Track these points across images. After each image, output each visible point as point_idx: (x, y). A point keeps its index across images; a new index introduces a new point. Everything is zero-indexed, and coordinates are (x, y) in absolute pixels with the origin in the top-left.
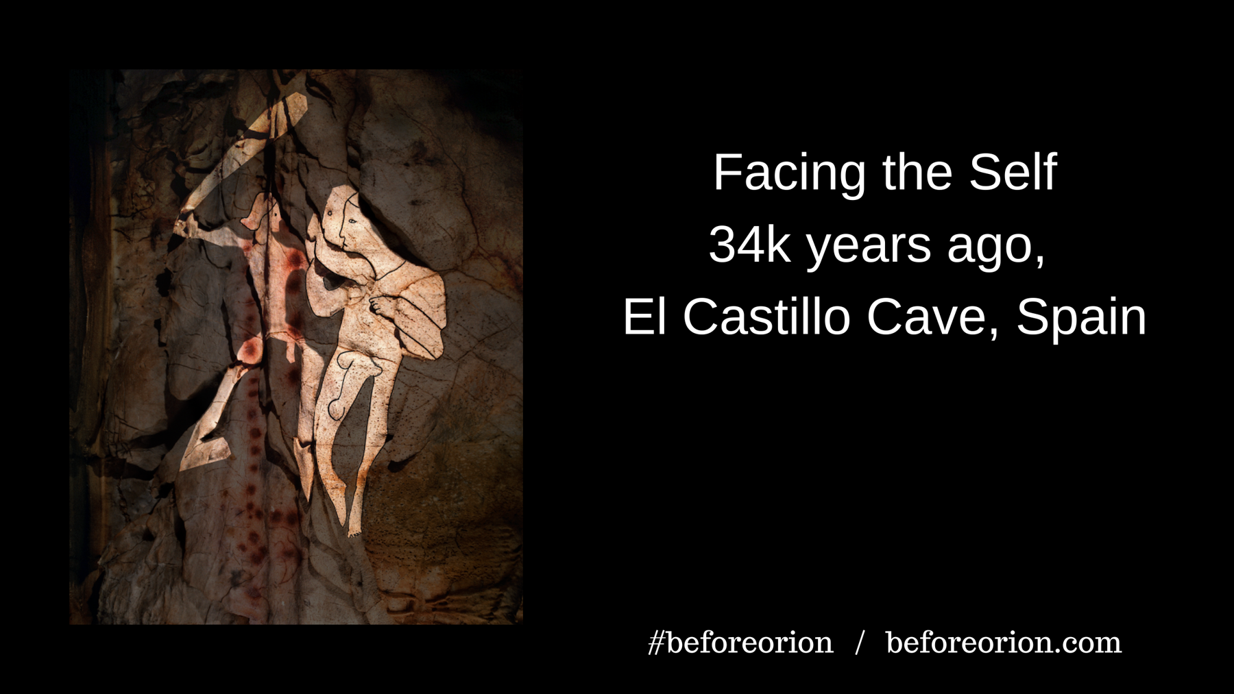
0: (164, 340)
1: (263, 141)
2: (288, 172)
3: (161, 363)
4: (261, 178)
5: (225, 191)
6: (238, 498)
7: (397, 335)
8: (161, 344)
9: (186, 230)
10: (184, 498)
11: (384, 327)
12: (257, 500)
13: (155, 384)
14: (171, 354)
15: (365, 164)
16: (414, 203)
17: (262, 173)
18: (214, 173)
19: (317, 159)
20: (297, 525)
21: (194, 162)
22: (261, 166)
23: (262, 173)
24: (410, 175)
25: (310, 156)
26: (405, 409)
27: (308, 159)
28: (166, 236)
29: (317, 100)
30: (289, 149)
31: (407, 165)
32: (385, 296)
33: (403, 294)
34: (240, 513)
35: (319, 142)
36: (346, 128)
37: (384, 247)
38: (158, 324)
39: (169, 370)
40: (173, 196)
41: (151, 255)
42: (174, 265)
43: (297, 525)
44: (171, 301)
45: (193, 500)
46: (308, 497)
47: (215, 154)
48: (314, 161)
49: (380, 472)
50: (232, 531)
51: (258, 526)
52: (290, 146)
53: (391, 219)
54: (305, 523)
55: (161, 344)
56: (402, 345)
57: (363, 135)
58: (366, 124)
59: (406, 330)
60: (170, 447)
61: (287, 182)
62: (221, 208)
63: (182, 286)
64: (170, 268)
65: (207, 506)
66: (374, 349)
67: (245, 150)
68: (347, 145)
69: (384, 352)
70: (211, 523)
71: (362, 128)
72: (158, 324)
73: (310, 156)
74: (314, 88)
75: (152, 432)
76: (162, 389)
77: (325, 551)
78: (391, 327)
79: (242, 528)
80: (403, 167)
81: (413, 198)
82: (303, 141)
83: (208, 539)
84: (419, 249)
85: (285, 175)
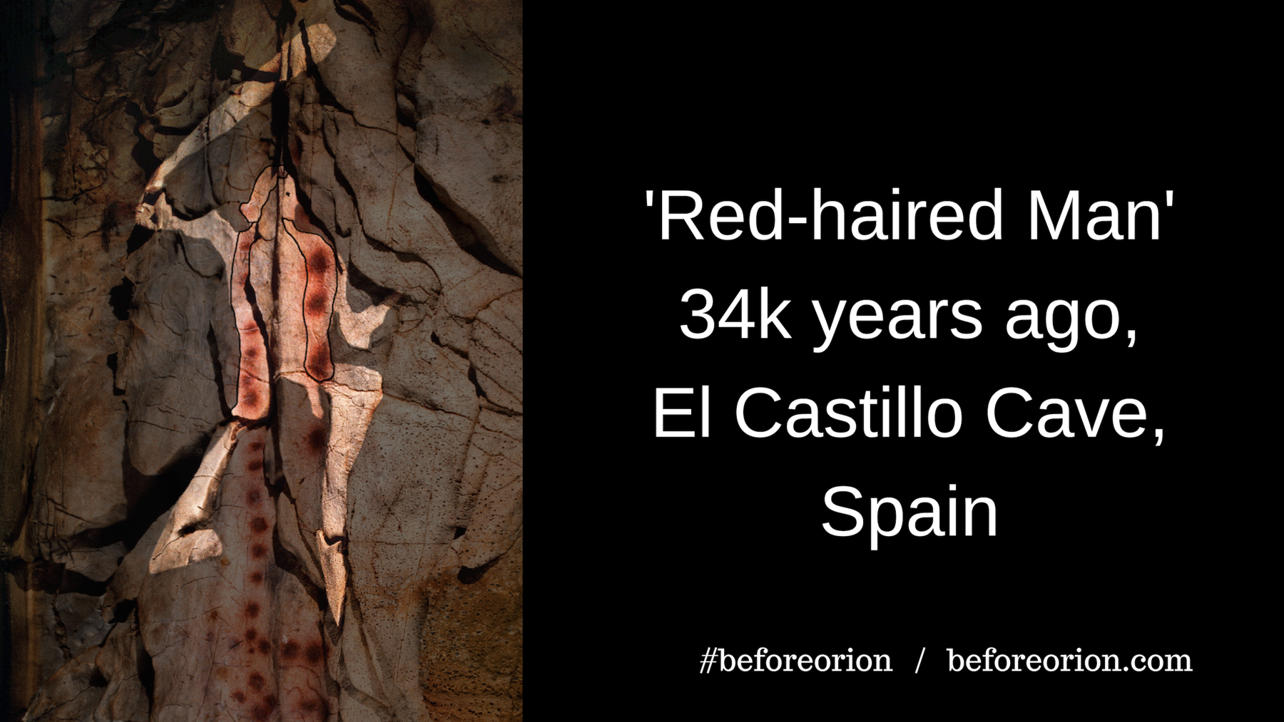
0: (121, 386)
1: (270, 86)
2: (307, 132)
3: (117, 420)
4: (268, 142)
5: (213, 162)
6: (233, 623)
7: (472, 376)
8: (118, 392)
9: (155, 219)
10: (152, 622)
11: (453, 365)
12: (261, 625)
13: (109, 451)
14: (133, 407)
15: (422, 122)
16: (497, 179)
17: (269, 135)
18: (196, 132)
19: (351, 113)
20: (321, 663)
21: (167, 118)
22: (268, 123)
23: (269, 135)
24: (490, 138)
25: (341, 108)
26: (484, 488)
27: (337, 114)
28: (125, 229)
29: (352, 26)
30: (310, 99)
31: (486, 122)
32: (454, 317)
33: (482, 315)
34: (235, 645)
35: (353, 89)
36: (395, 67)
37: (454, 244)
38: (113, 362)
39: (130, 430)
40: (136, 168)
41: (102, 258)
42: (137, 272)
43: (321, 663)
44: (132, 327)
45: (165, 625)
46: (338, 619)
47: (199, 106)
48: (347, 117)
49: (446, 583)
50: (223, 672)
51: (262, 664)
52: (311, 94)
53: (462, 204)
54: (334, 660)
55: (118, 392)
56: (480, 392)
57: (421, 77)
58: (425, 61)
59: (486, 369)
60: (130, 545)
61: (307, 147)
62: (208, 186)
63: (148, 304)
64: (131, 277)
65: (186, 634)
66: (437, 399)
67: (243, 98)
68: (396, 92)
69: (453, 404)
70: (192, 660)
71: (419, 67)
72: (113, 362)
73: (341, 108)
74: (346, 7)
75: (105, 523)
76: (119, 458)
77: (363, 702)
78: (464, 365)
79: (238, 668)
80: (481, 126)
81: (495, 173)
82: (330, 87)
83: (187, 684)
84: (504, 249)
85: (304, 138)
